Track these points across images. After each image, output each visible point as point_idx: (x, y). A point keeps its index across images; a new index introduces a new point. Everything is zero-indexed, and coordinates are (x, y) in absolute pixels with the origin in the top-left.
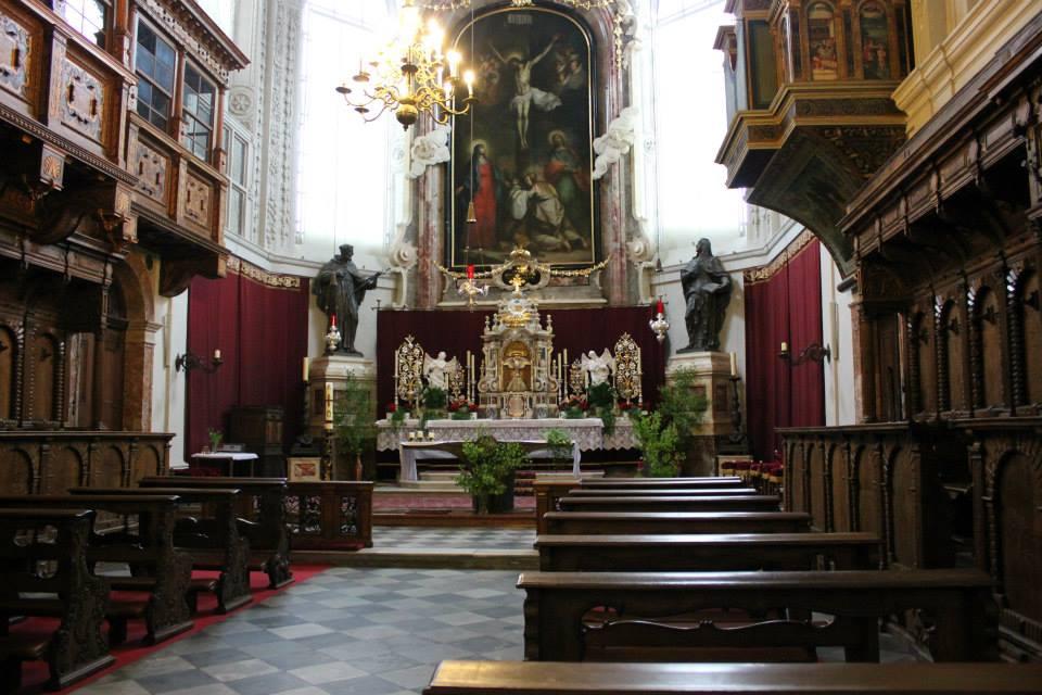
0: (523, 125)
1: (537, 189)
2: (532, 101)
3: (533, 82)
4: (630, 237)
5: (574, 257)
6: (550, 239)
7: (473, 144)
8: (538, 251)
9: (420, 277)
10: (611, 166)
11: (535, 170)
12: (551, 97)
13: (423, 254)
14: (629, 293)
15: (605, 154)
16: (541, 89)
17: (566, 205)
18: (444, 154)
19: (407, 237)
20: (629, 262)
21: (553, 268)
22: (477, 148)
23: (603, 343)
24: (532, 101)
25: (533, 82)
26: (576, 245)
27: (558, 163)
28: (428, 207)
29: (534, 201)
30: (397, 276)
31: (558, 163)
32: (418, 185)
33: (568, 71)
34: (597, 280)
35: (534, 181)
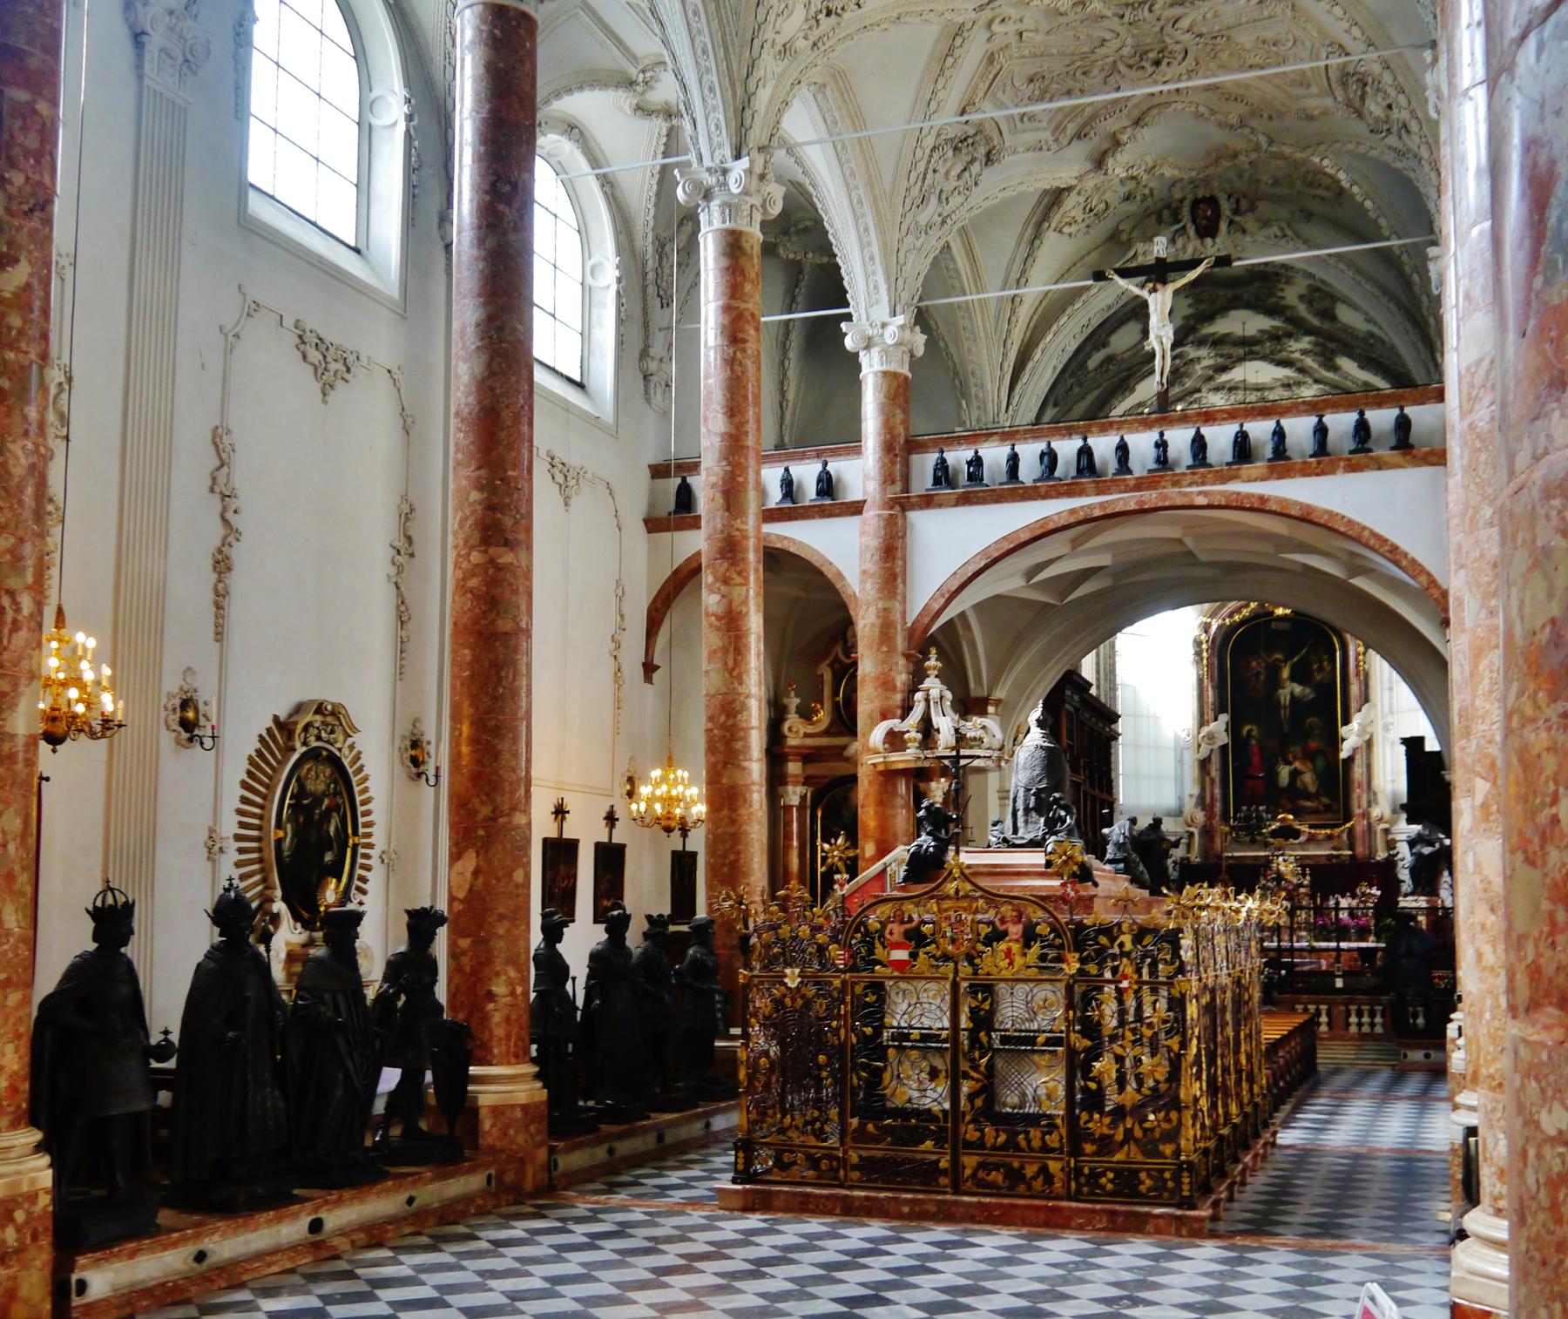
0: (1285, 714)
1: (1297, 764)
2: (1292, 693)
3: (1293, 678)
4: (1369, 805)
5: (1327, 818)
6: (1308, 804)
7: (1247, 728)
8: (1299, 813)
9: (1207, 832)
10: (1355, 750)
11: (1297, 749)
12: (1308, 691)
13: (1210, 816)
14: (1370, 847)
15: (1350, 737)
16: (1300, 683)
17: (1319, 776)
18: (1224, 739)
19: (1196, 806)
20: (1369, 825)
21: (1311, 827)
22: (1250, 731)
23: (1348, 889)
24: (1292, 693)
25: (1293, 678)
26: (1328, 809)
27: (1313, 744)
28: (1213, 781)
29: (1295, 774)
30: (1191, 835)
31: (1313, 744)
32: (1204, 764)
33: (1321, 669)
34: (1345, 836)
35: (1295, 758)
